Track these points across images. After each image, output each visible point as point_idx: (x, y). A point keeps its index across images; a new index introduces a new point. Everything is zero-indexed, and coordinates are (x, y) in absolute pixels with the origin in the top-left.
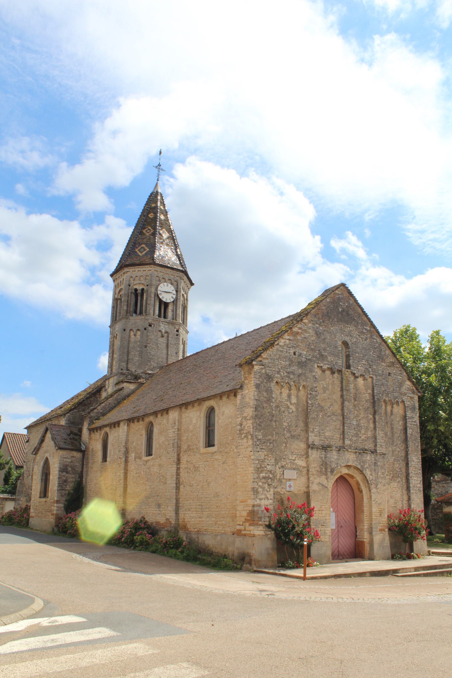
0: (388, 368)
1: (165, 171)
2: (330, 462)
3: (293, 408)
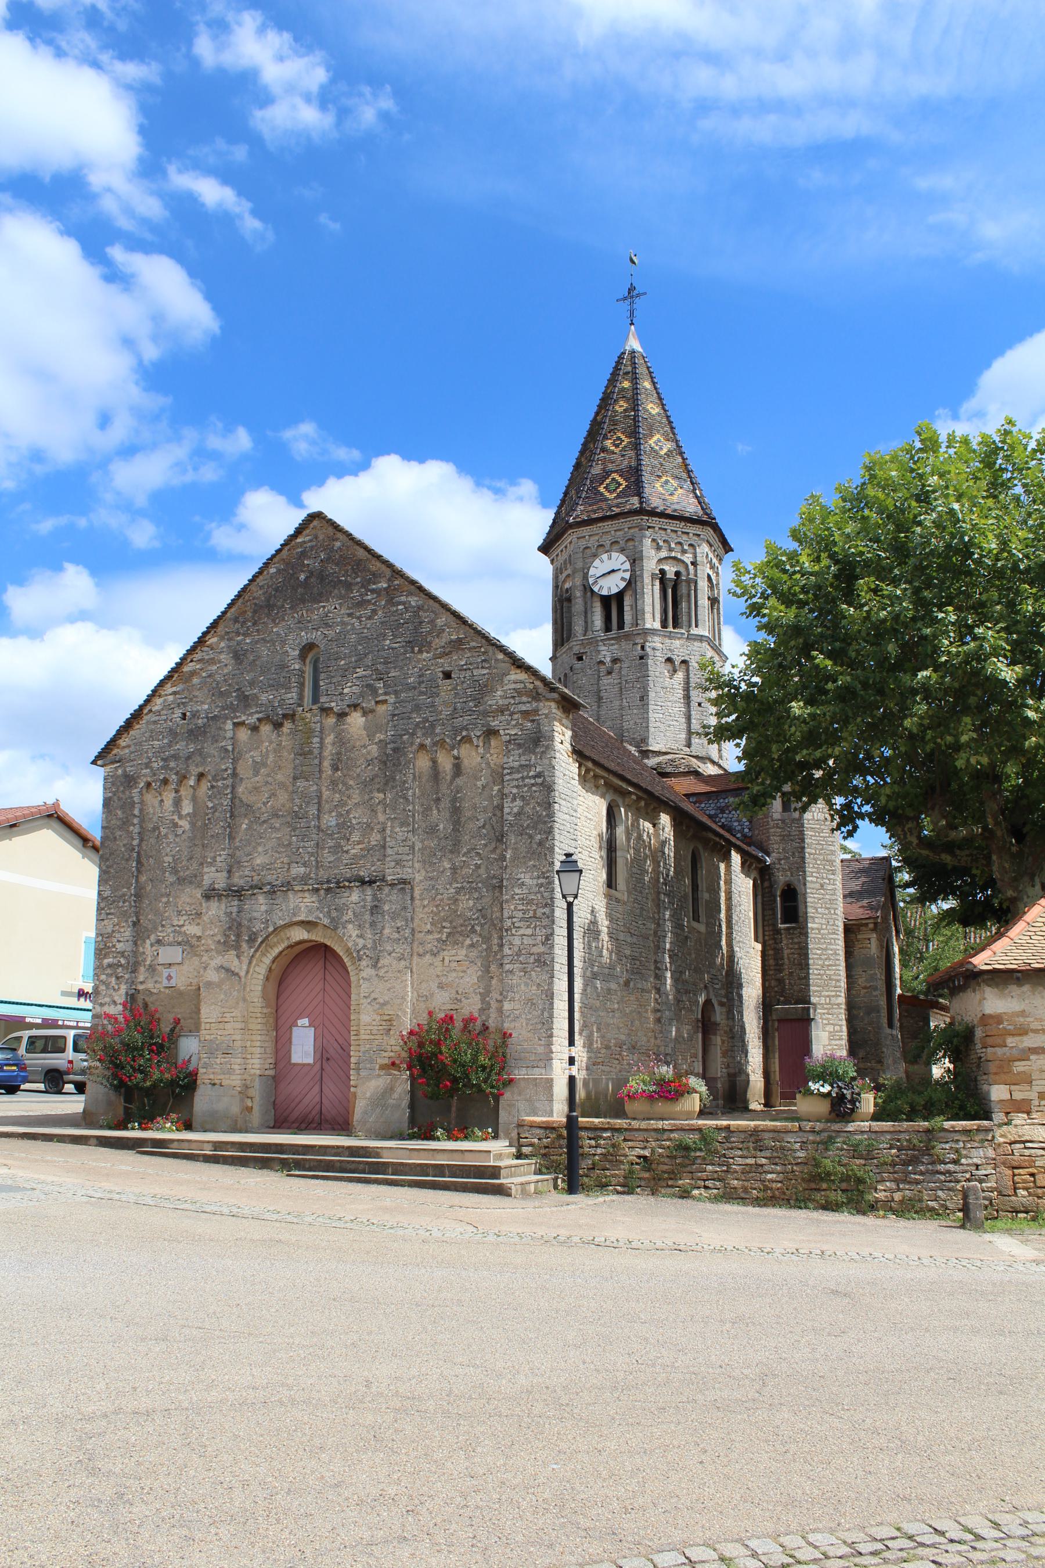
0: (440, 661)
1: (645, 293)
2: (250, 920)
3: (185, 824)
